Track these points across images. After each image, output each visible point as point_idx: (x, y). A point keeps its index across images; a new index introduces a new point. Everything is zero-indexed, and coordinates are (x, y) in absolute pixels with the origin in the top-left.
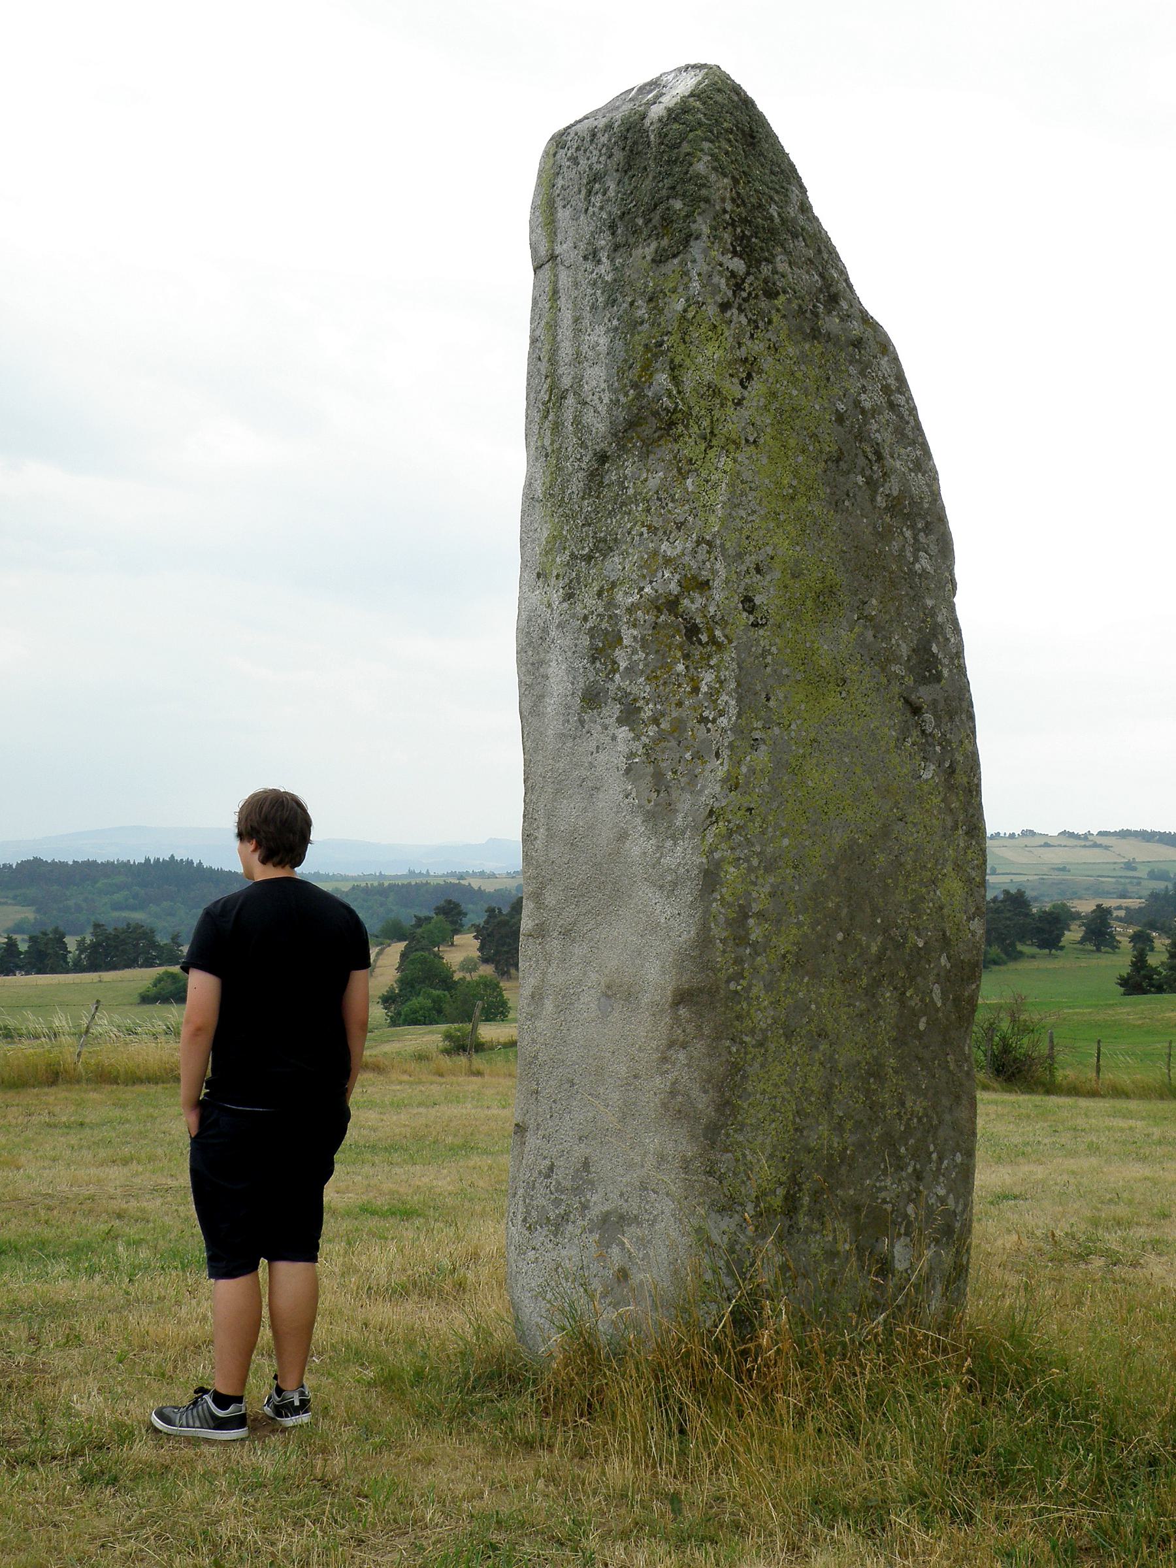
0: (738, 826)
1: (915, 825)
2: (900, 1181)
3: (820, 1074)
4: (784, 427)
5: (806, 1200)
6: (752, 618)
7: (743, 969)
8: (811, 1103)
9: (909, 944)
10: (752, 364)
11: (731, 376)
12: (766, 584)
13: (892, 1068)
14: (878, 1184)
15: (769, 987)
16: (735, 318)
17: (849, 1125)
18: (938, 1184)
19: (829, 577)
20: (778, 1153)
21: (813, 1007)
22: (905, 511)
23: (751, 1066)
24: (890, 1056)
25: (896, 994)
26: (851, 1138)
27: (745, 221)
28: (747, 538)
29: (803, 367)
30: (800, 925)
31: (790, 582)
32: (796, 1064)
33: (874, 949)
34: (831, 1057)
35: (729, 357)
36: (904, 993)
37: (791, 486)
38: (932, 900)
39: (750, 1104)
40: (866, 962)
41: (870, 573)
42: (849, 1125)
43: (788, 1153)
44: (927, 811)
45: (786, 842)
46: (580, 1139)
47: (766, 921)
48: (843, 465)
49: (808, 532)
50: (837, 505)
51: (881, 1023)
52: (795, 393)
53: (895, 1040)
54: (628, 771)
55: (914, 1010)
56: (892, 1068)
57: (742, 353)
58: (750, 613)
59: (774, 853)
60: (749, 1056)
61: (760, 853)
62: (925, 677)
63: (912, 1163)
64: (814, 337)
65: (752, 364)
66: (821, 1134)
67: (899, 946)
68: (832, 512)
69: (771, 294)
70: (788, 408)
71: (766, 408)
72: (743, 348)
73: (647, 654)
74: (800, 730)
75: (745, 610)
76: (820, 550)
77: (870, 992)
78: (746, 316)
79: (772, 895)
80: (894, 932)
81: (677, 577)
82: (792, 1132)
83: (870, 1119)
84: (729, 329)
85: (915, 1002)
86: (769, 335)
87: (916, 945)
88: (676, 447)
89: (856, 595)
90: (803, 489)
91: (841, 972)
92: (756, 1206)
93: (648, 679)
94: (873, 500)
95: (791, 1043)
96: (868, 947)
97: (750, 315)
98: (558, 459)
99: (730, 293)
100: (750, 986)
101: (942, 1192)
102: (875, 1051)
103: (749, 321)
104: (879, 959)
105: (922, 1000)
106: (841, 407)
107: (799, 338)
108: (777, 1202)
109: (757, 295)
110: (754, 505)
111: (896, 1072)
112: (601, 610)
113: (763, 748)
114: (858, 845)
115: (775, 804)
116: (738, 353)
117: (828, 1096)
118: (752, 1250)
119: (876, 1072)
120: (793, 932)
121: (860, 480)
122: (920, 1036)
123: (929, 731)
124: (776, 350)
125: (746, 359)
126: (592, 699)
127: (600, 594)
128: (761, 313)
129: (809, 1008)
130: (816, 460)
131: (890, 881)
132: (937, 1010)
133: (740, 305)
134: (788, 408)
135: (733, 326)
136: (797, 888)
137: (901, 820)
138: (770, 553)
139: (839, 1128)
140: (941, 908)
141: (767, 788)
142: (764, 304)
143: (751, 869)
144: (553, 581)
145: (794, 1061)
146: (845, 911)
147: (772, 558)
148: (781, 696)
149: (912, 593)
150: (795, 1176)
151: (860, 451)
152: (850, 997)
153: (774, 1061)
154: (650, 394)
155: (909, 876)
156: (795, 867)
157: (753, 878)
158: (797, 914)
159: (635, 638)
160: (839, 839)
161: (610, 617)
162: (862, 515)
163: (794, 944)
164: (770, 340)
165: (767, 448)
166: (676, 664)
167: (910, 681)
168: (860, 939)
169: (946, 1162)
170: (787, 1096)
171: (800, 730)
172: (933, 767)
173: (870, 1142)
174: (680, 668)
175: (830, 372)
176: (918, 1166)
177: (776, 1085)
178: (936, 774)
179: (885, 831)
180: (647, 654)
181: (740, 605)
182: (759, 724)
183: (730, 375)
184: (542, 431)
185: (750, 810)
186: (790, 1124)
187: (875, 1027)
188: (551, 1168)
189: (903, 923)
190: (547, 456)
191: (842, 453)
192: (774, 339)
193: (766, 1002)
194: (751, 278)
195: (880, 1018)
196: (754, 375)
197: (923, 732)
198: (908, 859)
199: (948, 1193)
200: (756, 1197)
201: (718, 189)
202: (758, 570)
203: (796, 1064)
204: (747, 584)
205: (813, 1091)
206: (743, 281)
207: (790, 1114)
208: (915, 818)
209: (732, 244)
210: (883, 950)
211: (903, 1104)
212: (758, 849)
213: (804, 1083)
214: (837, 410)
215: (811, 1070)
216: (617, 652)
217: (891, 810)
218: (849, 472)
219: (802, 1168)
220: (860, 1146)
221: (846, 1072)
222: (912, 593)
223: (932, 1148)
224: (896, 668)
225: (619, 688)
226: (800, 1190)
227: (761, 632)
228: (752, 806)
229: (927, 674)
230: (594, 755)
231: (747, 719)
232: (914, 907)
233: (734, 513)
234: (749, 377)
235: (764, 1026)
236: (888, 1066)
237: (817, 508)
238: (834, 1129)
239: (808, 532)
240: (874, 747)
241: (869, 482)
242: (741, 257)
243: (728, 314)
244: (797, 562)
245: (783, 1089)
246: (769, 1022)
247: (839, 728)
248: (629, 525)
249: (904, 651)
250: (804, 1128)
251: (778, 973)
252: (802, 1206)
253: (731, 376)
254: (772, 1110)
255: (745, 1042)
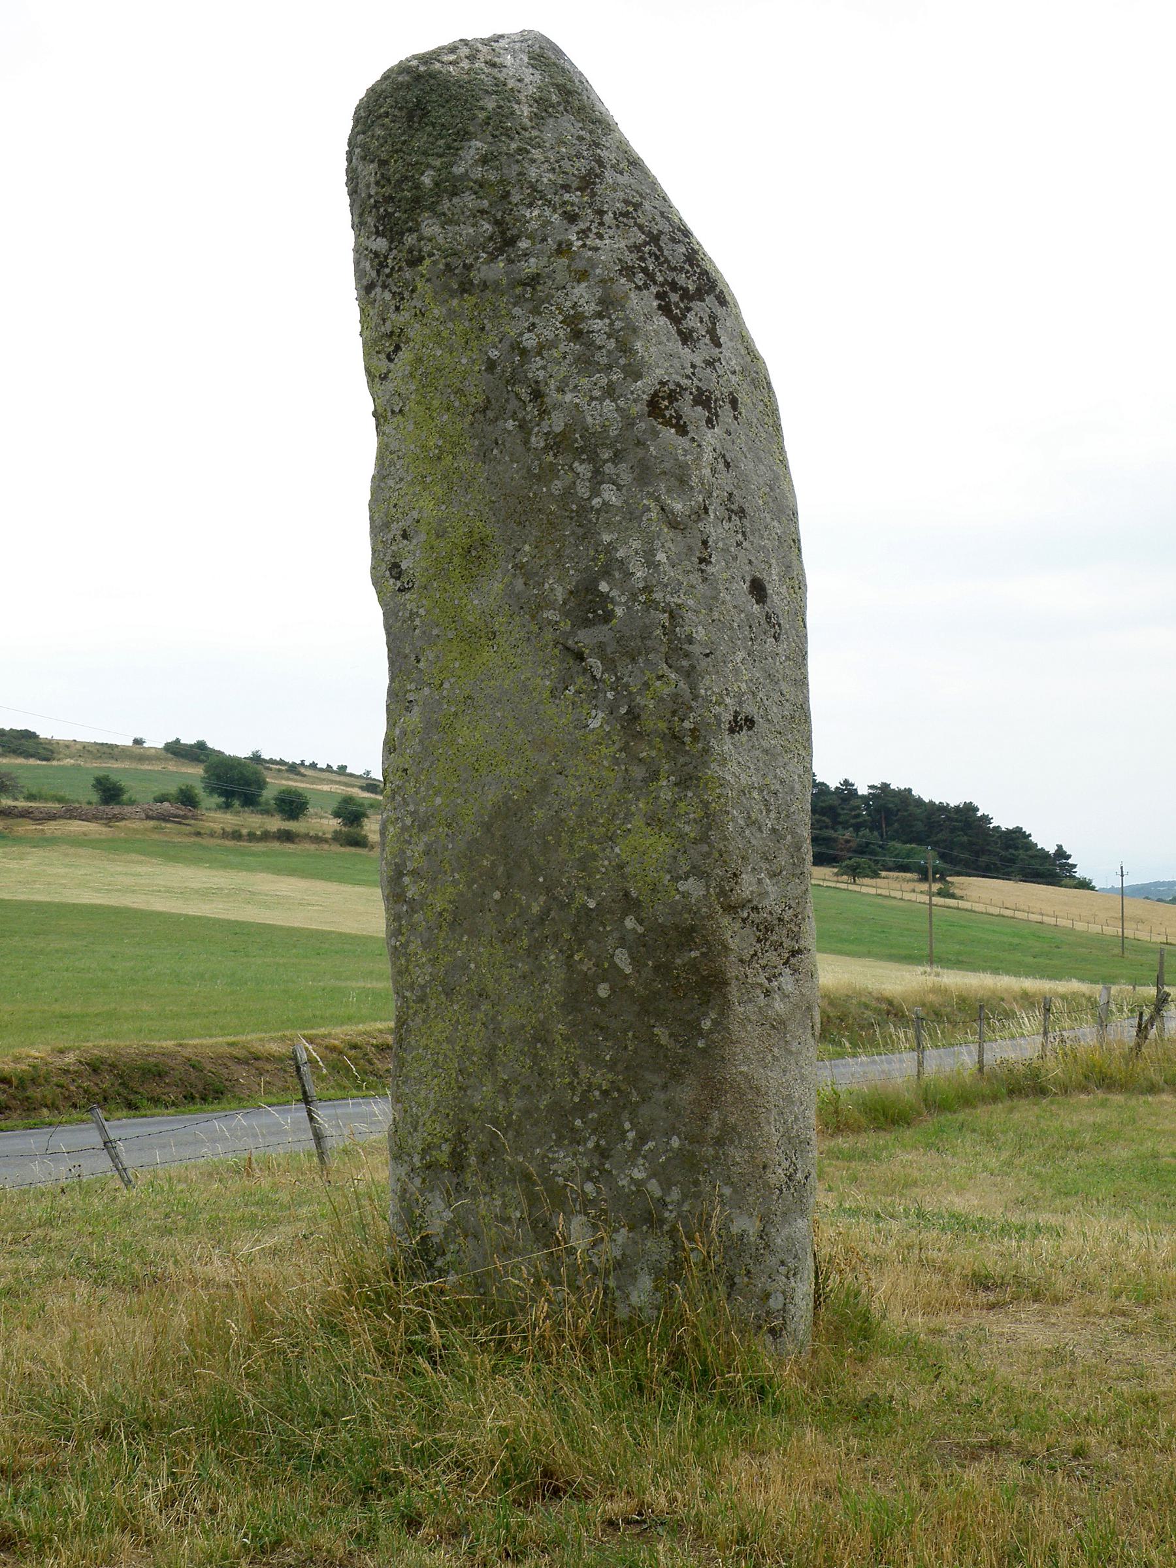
0: (399, 787)
1: (577, 778)
2: (575, 1154)
3: (481, 1034)
4: (429, 389)
5: (473, 1160)
6: (399, 584)
7: (400, 925)
8: (473, 1063)
9: (577, 905)
10: (399, 336)
11: (378, 352)
12: (412, 548)
13: (561, 1035)
14: (550, 1155)
15: (426, 945)
16: (378, 298)
17: (515, 1090)
18: (635, 1165)
19: (477, 530)
20: (441, 1109)
21: (472, 966)
22: (576, 445)
23: (413, 1021)
24: (559, 1022)
25: (562, 957)
26: (518, 1104)
27: (389, 199)
28: (395, 507)
29: (450, 325)
30: (455, 883)
31: (436, 543)
32: (457, 1021)
33: (535, 909)
34: (494, 1018)
35: (375, 335)
36: (571, 956)
37: (437, 447)
38: (607, 858)
39: (413, 1058)
40: (525, 923)
41: (523, 518)
42: (515, 1090)
43: (452, 1110)
44: (593, 762)
45: (438, 800)
47: (422, 879)
48: (490, 414)
49: (455, 488)
50: (484, 455)
51: (547, 986)
52: (439, 353)
53: (564, 1005)
55: (586, 974)
56: (561, 1035)
57: (388, 327)
58: (398, 578)
59: (427, 813)
60: (411, 1011)
61: (413, 812)
62: (587, 619)
63: (594, 1138)
64: (464, 291)
65: (399, 336)
66: (483, 1093)
67: (564, 907)
68: (480, 464)
69: (415, 262)
70: (432, 370)
71: (411, 375)
72: (388, 323)
74: (453, 689)
75: (392, 577)
76: (467, 505)
77: (534, 951)
78: (390, 291)
79: (426, 853)
80: (559, 891)
82: (456, 1089)
83: (538, 1086)
84: (374, 308)
85: (587, 966)
86: (414, 303)
87: (584, 906)
89: (510, 544)
90: (449, 446)
91: (499, 932)
92: (422, 1159)
94: (526, 442)
95: (452, 1001)
96: (529, 907)
97: (394, 289)
99: (374, 274)
100: (408, 942)
101: (638, 1175)
102: (541, 1016)
103: (394, 294)
104: (542, 919)
105: (596, 965)
106: (494, 354)
107: (446, 296)
108: (443, 1155)
109: (400, 269)
110: (401, 473)
111: (566, 1039)
113: (416, 709)
114: (513, 801)
115: (426, 765)
116: (383, 329)
117: (491, 1057)
118: (420, 1201)
119: (541, 1037)
120: (449, 890)
121: (510, 424)
122: (602, 1003)
123: (598, 677)
124: (423, 315)
125: (392, 332)
128: (406, 284)
129: (468, 967)
130: (462, 415)
131: (550, 838)
132: (626, 977)
133: (384, 282)
134: (432, 370)
135: (377, 305)
136: (450, 846)
137: (561, 773)
138: (416, 517)
139: (504, 1090)
140: (621, 867)
141: (418, 749)
142: (408, 274)
143: (404, 829)
145: (455, 1019)
146: (501, 869)
147: (418, 521)
148: (431, 656)
149: (580, 531)
150: (460, 1134)
151: (512, 394)
152: (511, 958)
153: (436, 1017)
155: (574, 832)
156: (449, 826)
157: (406, 836)
158: (453, 871)
160: (493, 796)
162: (511, 461)
163: (450, 902)
164: (415, 307)
165: (413, 415)
167: (566, 626)
168: (520, 899)
169: (651, 1145)
170: (449, 1054)
171: (453, 689)
172: (601, 715)
173: (537, 1108)
175: (486, 321)
176: (603, 1142)
177: (437, 1041)
178: (606, 721)
179: (544, 786)
181: (388, 573)
182: (413, 686)
183: (377, 352)
185: (405, 770)
186: (453, 1082)
187: (540, 990)
189: (569, 883)
191: (489, 402)
192: (419, 305)
193: (424, 960)
194: (395, 252)
195: (545, 982)
196: (402, 345)
197: (594, 677)
198: (570, 815)
199: (649, 1178)
200: (422, 1150)
201: (365, 177)
202: (405, 536)
203: (457, 1021)
204: (393, 551)
205: (474, 1051)
206: (386, 257)
207: (453, 1071)
208: (577, 770)
209: (375, 226)
210: (546, 912)
211: (576, 1074)
212: (411, 808)
213: (466, 1041)
214: (489, 358)
215: (472, 1030)
217: (550, 763)
218: (497, 419)
219: (467, 1128)
220: (527, 1113)
221: (511, 1034)
222: (580, 531)
223: (627, 1126)
224: (549, 614)
226: (466, 1149)
227: (408, 596)
228: (406, 767)
229: (590, 615)
231: (400, 682)
232: (585, 863)
233: (382, 485)
234: (398, 348)
235: (423, 982)
236: (556, 1032)
237: (463, 463)
238: (499, 1092)
239: (455, 488)
240: (525, 699)
241: (523, 426)
242: (383, 236)
243: (372, 295)
244: (441, 520)
245: (445, 1046)
246: (427, 978)
247: (493, 682)
249: (560, 594)
250: (467, 1087)
251: (436, 931)
252: (469, 1165)
253: (378, 352)
254: (434, 1066)
255: (406, 997)
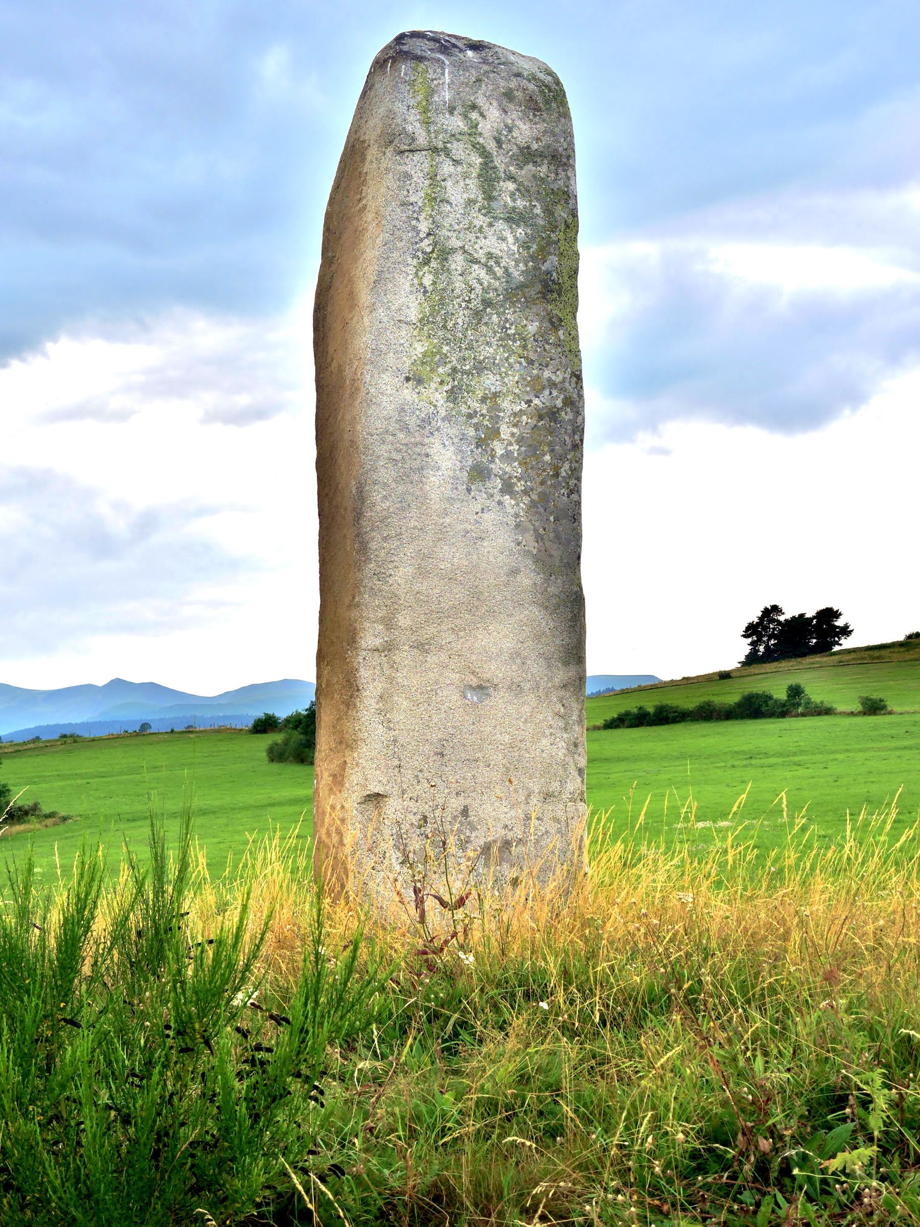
46: (457, 793)
54: (517, 526)
73: (521, 446)
81: (562, 396)
88: (550, 307)
93: (519, 464)
98: (442, 298)
112: (484, 412)
126: (479, 473)
127: (483, 400)
144: (433, 385)
154: (543, 268)
159: (513, 434)
161: (491, 417)
166: (544, 455)
174: (547, 458)
180: (521, 446)
184: (421, 273)
188: (425, 819)
190: (425, 292)
216: (495, 443)
225: (500, 468)
230: (480, 514)
248: (506, 355)
